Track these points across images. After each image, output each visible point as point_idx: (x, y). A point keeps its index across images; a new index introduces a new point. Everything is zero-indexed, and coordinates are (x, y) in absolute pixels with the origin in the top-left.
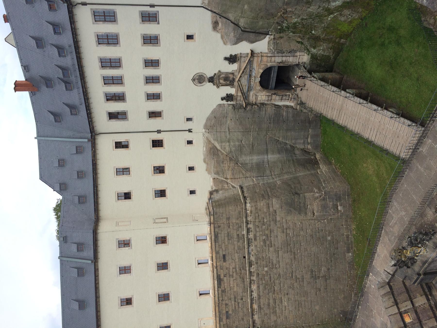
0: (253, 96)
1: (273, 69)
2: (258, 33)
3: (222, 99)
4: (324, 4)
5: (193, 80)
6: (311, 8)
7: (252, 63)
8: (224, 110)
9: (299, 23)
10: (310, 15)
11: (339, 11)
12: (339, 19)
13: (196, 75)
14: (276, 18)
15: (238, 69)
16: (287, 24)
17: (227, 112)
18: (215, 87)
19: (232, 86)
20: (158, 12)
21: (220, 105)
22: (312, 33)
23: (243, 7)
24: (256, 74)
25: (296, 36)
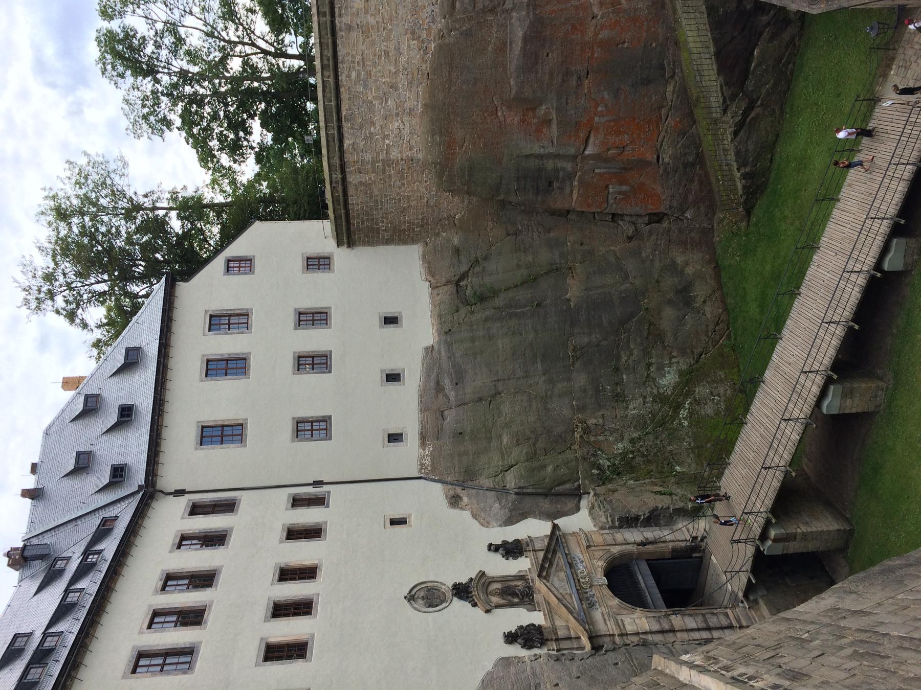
0: (605, 619)
1: (636, 568)
2: (553, 495)
3: (511, 638)
4: (649, 389)
5: (411, 598)
6: (630, 407)
7: (563, 540)
8: (525, 671)
9: (632, 452)
10: (640, 423)
11: (687, 396)
12: (703, 413)
13: (419, 587)
14: (576, 447)
15: (532, 564)
16: (608, 459)
17: (534, 674)
18: (479, 612)
19: (529, 606)
20: (329, 492)
21: (506, 662)
22: (677, 472)
23: (501, 443)
24: (589, 567)
25: (645, 483)
